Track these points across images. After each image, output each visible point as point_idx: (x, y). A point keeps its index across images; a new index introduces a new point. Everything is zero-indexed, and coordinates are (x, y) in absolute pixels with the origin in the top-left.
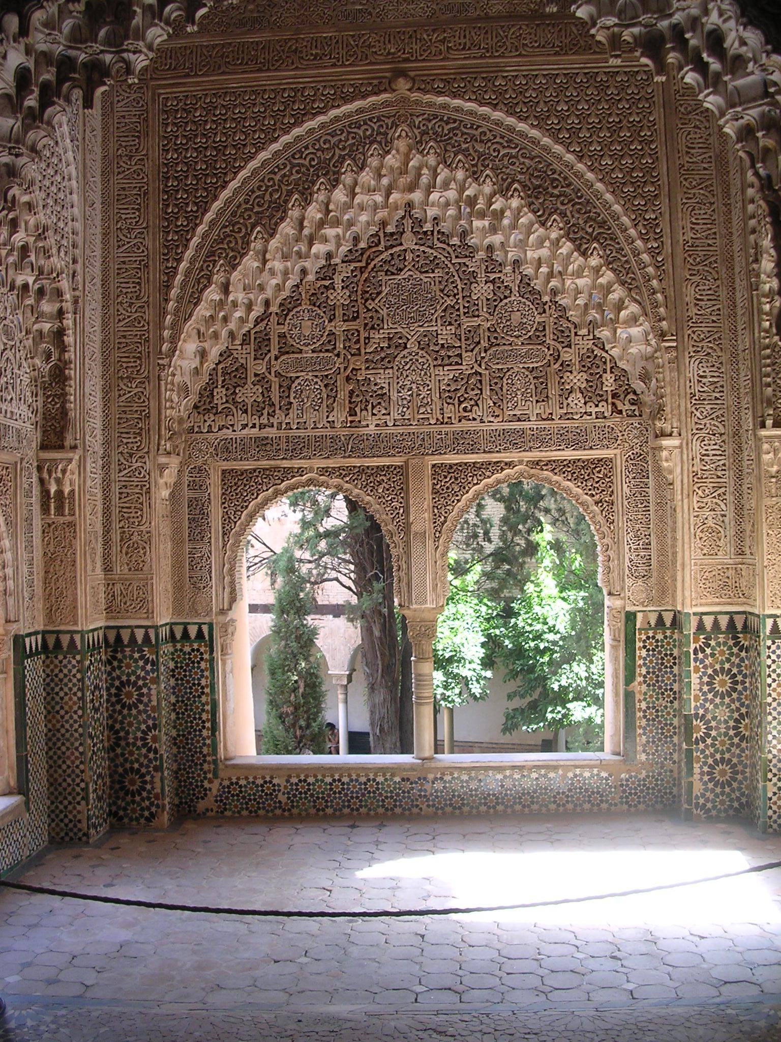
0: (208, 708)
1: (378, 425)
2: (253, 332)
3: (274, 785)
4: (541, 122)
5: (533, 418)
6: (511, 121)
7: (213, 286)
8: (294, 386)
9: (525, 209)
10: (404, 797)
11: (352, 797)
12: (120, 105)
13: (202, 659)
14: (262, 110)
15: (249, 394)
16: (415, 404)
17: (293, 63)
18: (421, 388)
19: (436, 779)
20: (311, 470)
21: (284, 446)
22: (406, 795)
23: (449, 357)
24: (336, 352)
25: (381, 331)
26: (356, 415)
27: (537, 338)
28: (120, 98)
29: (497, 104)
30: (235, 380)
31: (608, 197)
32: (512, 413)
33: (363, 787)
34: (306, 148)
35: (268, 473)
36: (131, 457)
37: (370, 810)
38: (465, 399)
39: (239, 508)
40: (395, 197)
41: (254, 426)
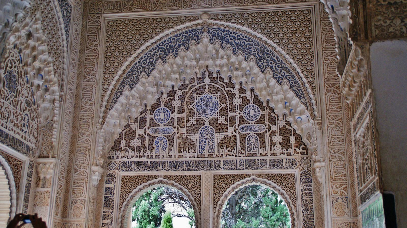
1: (190, 157)
4: (263, 31)
5: (259, 155)
6: (250, 31)
7: (123, 96)
9: (256, 66)
12: (90, 23)
14: (148, 26)
15: (136, 143)
17: (161, 8)
20: (161, 176)
21: (149, 165)
23: (223, 129)
24: (174, 126)
26: (181, 153)
27: (262, 120)
28: (90, 20)
29: (244, 24)
31: (291, 61)
34: (165, 41)
36: (81, 167)
38: (229, 147)
39: (127, 193)
40: (201, 62)
41: (137, 157)
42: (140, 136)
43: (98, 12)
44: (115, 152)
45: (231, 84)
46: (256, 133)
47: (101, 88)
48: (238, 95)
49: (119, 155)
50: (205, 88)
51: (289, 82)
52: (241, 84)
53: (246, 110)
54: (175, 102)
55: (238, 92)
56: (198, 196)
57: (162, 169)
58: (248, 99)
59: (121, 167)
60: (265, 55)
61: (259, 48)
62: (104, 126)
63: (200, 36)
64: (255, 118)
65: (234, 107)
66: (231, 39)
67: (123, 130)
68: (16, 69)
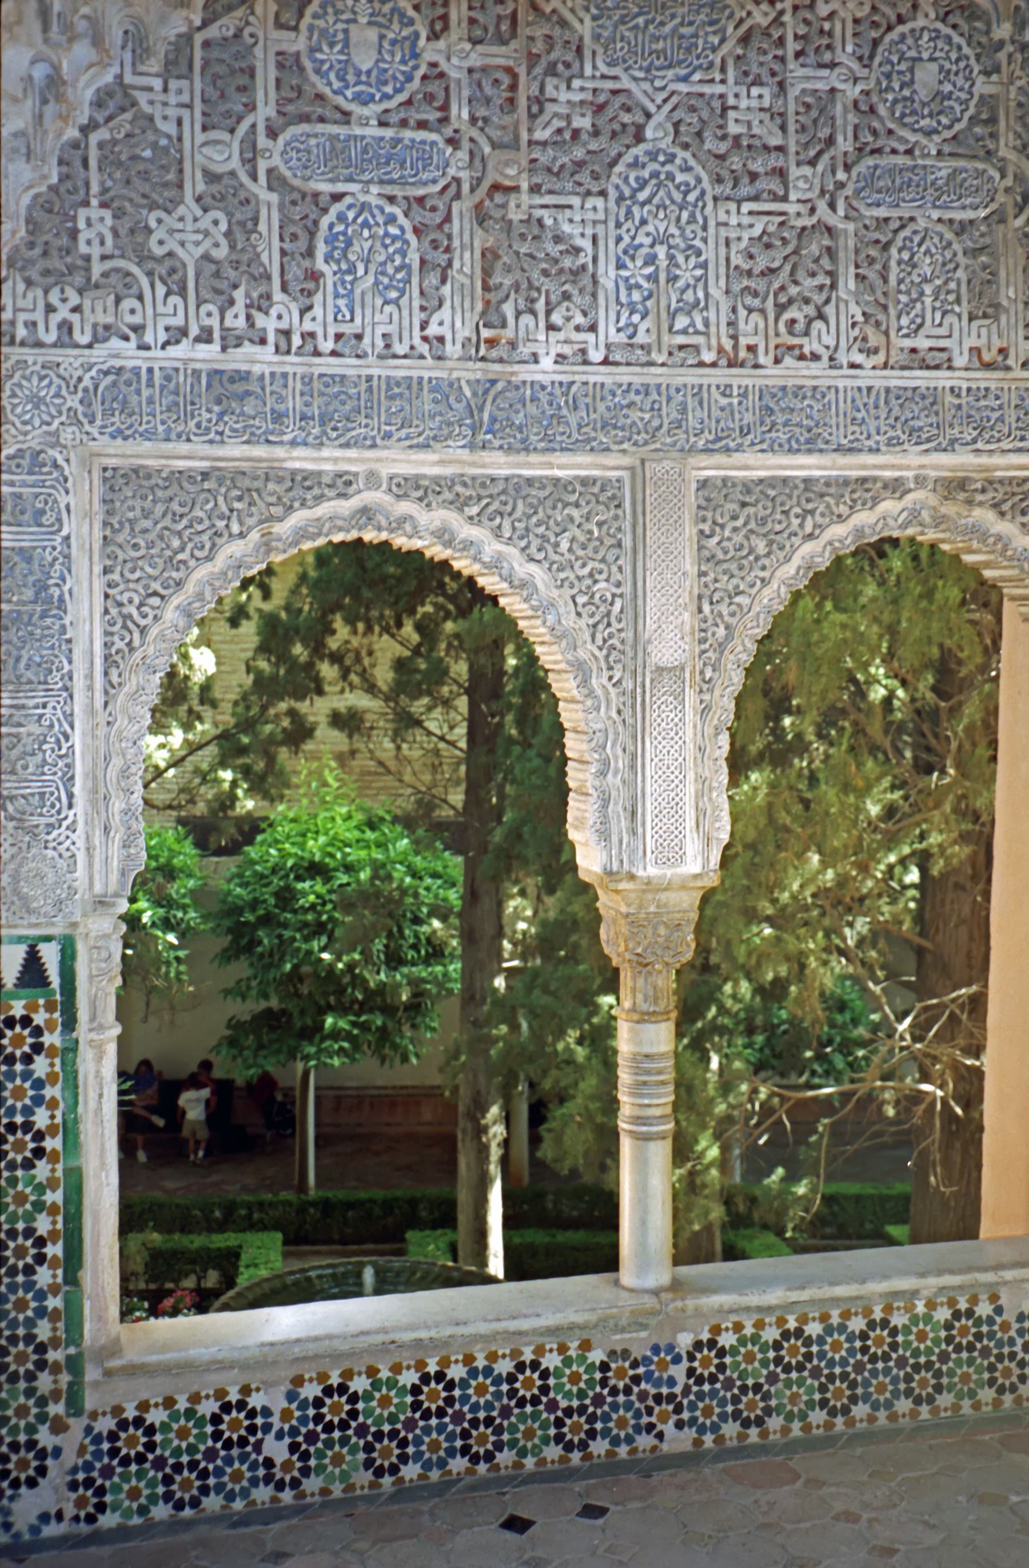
0: (55, 1197)
2: (199, 38)
3: (252, 1414)
5: (960, 361)
8: (325, 222)
10: (615, 1407)
11: (475, 1423)
13: (37, 1048)
16: (663, 304)
18: (680, 259)
19: (698, 1345)
20: (372, 479)
21: (294, 403)
22: (621, 1398)
23: (754, 176)
24: (449, 132)
25: (576, 83)
26: (504, 325)
30: (146, 188)
32: (908, 343)
33: (505, 1387)
35: (246, 483)
37: (523, 1453)
38: (791, 301)
41: (205, 337)
42: (215, 188)
44: (40, 292)
46: (947, 215)
49: (75, 318)
53: (895, 59)
56: (608, 614)
57: (388, 436)
59: (98, 408)
64: (945, 121)
65: (822, 31)
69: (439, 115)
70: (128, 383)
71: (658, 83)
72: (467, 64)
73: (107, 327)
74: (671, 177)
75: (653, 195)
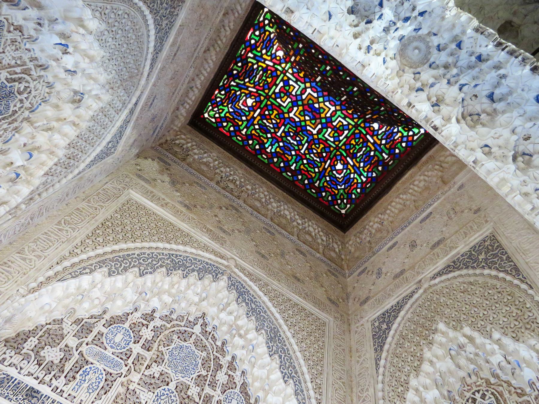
4: (281, 312)
6: (270, 304)
7: (91, 276)
8: (86, 367)
9: (264, 345)
24: (126, 363)
31: (302, 362)
34: (180, 256)
40: (205, 303)
41: (37, 378)
42: (66, 349)
43: (127, 184)
45: (222, 350)
47: (70, 248)
48: (226, 369)
49: (9, 358)
50: (191, 337)
51: (295, 385)
52: (233, 358)
54: (146, 330)
55: (227, 365)
58: (235, 381)
60: (277, 338)
61: (273, 327)
62: (31, 296)
63: (219, 275)
66: (248, 299)
67: (47, 324)
68: (19, 105)
69: (126, 358)
70: (8, 379)
71: (177, 375)
72: (138, 351)
73: (14, 365)
74: (171, 396)
75: (165, 398)
